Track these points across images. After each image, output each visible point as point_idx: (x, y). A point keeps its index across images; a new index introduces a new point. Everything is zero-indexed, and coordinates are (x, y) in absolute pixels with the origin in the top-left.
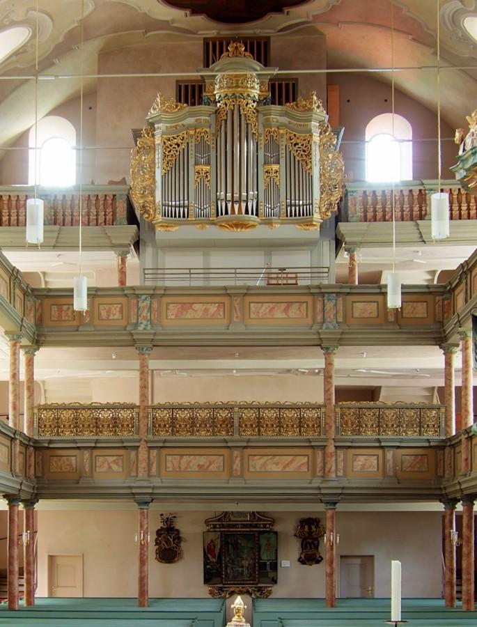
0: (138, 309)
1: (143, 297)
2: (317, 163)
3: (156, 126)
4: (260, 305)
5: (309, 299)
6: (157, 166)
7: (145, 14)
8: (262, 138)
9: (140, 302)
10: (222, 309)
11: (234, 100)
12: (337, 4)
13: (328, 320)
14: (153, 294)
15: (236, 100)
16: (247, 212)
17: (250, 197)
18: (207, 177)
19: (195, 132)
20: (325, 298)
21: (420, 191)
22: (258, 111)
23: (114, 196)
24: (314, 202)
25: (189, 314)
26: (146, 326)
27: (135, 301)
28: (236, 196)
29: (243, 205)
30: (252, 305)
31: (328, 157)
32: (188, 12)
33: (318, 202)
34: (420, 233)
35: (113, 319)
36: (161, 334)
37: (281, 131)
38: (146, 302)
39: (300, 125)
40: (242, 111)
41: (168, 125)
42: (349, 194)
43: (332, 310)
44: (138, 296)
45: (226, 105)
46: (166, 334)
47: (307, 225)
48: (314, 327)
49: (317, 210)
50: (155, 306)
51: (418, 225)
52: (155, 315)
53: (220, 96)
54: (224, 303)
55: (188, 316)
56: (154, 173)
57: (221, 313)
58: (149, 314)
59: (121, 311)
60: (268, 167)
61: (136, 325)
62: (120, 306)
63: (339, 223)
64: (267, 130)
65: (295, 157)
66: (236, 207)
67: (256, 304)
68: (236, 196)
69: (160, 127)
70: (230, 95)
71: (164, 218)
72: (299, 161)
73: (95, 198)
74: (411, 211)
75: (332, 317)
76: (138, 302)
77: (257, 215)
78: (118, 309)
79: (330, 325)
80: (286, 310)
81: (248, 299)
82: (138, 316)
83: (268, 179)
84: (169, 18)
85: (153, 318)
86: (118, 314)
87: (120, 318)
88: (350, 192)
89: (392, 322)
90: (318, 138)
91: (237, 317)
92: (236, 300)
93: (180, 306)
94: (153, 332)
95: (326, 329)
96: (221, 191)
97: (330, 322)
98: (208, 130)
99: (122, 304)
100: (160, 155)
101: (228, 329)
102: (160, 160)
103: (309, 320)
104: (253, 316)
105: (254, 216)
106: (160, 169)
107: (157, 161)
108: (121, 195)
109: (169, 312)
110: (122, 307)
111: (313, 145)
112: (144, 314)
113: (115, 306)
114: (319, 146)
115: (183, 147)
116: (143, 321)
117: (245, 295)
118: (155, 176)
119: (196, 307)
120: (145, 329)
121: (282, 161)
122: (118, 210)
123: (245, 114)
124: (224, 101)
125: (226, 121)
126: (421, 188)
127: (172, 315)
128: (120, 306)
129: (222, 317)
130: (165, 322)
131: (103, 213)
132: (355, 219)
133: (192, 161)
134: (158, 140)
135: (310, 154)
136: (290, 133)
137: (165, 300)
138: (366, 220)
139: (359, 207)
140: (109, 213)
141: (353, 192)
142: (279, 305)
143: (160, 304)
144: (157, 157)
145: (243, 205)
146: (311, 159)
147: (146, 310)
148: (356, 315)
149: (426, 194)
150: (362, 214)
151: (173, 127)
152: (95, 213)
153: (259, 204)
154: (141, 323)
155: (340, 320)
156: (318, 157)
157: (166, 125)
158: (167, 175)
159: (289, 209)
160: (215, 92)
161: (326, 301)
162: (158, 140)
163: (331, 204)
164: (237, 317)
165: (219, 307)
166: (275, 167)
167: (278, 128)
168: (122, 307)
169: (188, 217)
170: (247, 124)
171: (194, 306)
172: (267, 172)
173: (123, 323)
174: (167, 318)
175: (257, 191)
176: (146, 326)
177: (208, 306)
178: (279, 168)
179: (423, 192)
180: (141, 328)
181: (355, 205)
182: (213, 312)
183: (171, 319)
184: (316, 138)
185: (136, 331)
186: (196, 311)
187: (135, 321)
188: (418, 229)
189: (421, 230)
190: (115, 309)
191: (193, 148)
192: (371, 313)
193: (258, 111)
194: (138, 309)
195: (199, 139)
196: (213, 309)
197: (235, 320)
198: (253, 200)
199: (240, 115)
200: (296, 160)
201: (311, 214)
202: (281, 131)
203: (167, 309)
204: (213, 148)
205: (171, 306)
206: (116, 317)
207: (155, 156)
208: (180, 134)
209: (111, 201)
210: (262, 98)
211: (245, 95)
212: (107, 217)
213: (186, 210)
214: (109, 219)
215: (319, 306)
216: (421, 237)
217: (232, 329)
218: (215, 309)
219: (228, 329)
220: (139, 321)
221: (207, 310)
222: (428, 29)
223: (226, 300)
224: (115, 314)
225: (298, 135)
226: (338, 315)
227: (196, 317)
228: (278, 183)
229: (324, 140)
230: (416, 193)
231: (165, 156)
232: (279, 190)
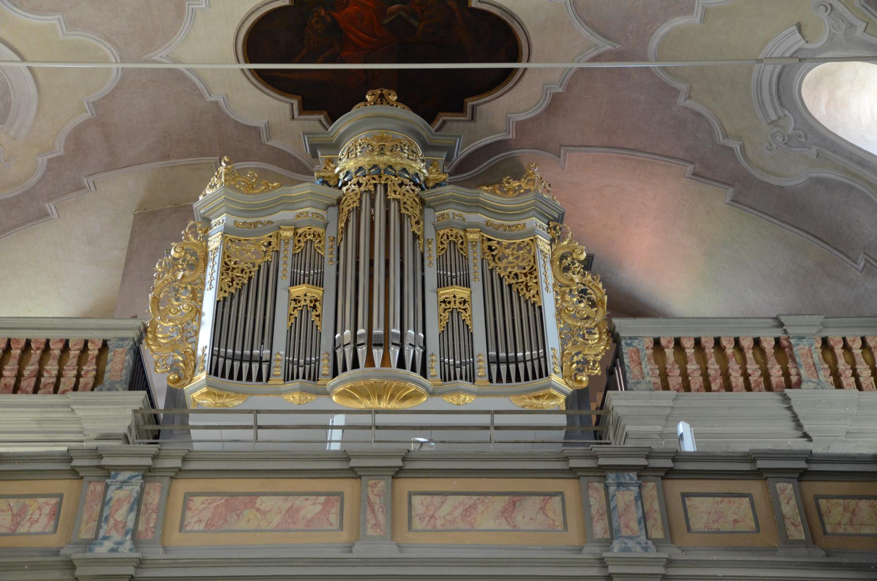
0: (105, 503)
1: (123, 476)
2: (551, 287)
3: (213, 222)
4: (437, 499)
5: (568, 487)
6: (208, 286)
7: (216, 103)
8: (433, 246)
9: (112, 488)
10: (335, 510)
11: (376, 177)
12: (560, 90)
13: (625, 532)
14: (150, 469)
15: (380, 177)
16: (401, 364)
17: (408, 340)
18: (315, 307)
19: (296, 234)
20: (610, 481)
21: (777, 341)
22: (423, 202)
23: (105, 344)
24: (550, 353)
25: (249, 519)
26: (121, 543)
27: (99, 488)
28: (378, 331)
29: (394, 352)
30: (416, 500)
31: (572, 280)
32: (295, 103)
33: (558, 355)
34: (795, 418)
35: (28, 534)
36: (156, 564)
37: (471, 236)
38: (127, 489)
39: (509, 226)
40: (392, 196)
41: (240, 220)
42: (623, 343)
43: (633, 509)
44: (107, 472)
45: (359, 184)
46: (175, 564)
47: (538, 398)
48: (587, 549)
49: (558, 370)
50: (154, 497)
51: (786, 399)
52: (148, 523)
53: (348, 173)
54: (340, 494)
55: (242, 525)
56: (201, 301)
57: (334, 518)
58: (132, 516)
59: (56, 514)
60: (447, 292)
61: (88, 544)
62: (54, 501)
63: (609, 392)
64: (441, 232)
65: (501, 279)
66: (378, 353)
67: (428, 498)
68: (378, 331)
69: (219, 222)
70: (367, 167)
71: (212, 377)
72: (510, 286)
73: (61, 346)
74: (766, 375)
75: (634, 525)
76: (107, 486)
77: (424, 374)
78: (46, 510)
79: (630, 544)
80: (507, 513)
81: (406, 485)
82: (102, 519)
83: (447, 314)
84: (260, 123)
85: (141, 527)
86: (44, 520)
87: (50, 529)
88: (625, 338)
89: (799, 542)
90: (548, 247)
91: (376, 525)
92: (374, 486)
93: (221, 501)
94: (137, 555)
95: (626, 549)
96: (343, 330)
97: (631, 538)
98: (320, 230)
99: (61, 496)
100: (216, 267)
101: (351, 552)
102: (215, 275)
103: (573, 536)
104: (417, 524)
105: (417, 376)
106: (213, 290)
107: (208, 279)
108: (123, 339)
109: (189, 514)
110: (59, 505)
111: (539, 257)
112: (119, 515)
113: (41, 500)
114: (552, 262)
115: (269, 258)
116: (114, 533)
117: (398, 473)
118: (201, 307)
119: (265, 503)
120: (113, 550)
121: (476, 285)
122: (108, 367)
123: (399, 201)
124: (354, 180)
125: (358, 210)
126: (778, 333)
127: (200, 521)
128: (54, 501)
129: (336, 526)
130: (175, 538)
131: (75, 372)
132: (642, 386)
133: (284, 282)
134: (215, 242)
135: (532, 271)
136: (490, 240)
137: (183, 486)
138: (666, 387)
139: (649, 368)
140: (87, 372)
141: (630, 338)
142: (487, 500)
143: (168, 494)
144: (209, 270)
145: (394, 352)
146: (536, 278)
147: (126, 507)
148: (698, 524)
149: (791, 347)
150: (658, 380)
151: (250, 224)
152: (55, 372)
153: (428, 358)
154: (106, 538)
155: (657, 533)
156: (551, 280)
157: (235, 218)
158: (228, 303)
159: (494, 367)
160: (337, 170)
161: (612, 489)
162: (215, 242)
163: (587, 362)
164: (376, 525)
165: (325, 505)
166: (462, 292)
167: (465, 231)
168: (59, 505)
169: (268, 379)
170: (402, 216)
171: (259, 501)
172: (444, 302)
173: (52, 541)
174: (181, 528)
175: (424, 333)
176: (121, 543)
177: (299, 502)
178: (470, 297)
179: (785, 343)
180: (102, 550)
181: (640, 364)
182: (310, 516)
183: (192, 531)
184: (543, 244)
185: (89, 555)
186: (264, 513)
187: (90, 536)
188: (790, 408)
189: (797, 410)
190: (40, 509)
191: (289, 262)
192: (735, 521)
193: (423, 202)
194: (105, 503)
195: (302, 244)
196: (310, 508)
197: (370, 532)
198: (414, 346)
199: (387, 203)
200: (505, 283)
201: (543, 373)
202: (471, 236)
203: (186, 507)
204: (331, 261)
205: (197, 502)
206: (37, 528)
207: (205, 271)
208: (265, 236)
209: (96, 352)
210: (431, 184)
211: (398, 168)
212: (81, 380)
213: (265, 367)
214: (86, 384)
215: (596, 500)
216: (799, 426)
217: (360, 551)
218: (318, 508)
219: (351, 552)
220: (102, 533)
221: (292, 512)
222: (726, 136)
223: (346, 486)
224: (37, 521)
225: (505, 242)
226: (650, 523)
227: (264, 525)
228: (468, 322)
229: (559, 253)
230: (768, 345)
231: (226, 268)
232: (471, 336)
